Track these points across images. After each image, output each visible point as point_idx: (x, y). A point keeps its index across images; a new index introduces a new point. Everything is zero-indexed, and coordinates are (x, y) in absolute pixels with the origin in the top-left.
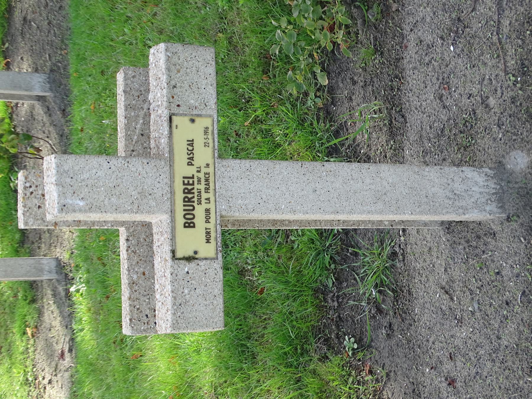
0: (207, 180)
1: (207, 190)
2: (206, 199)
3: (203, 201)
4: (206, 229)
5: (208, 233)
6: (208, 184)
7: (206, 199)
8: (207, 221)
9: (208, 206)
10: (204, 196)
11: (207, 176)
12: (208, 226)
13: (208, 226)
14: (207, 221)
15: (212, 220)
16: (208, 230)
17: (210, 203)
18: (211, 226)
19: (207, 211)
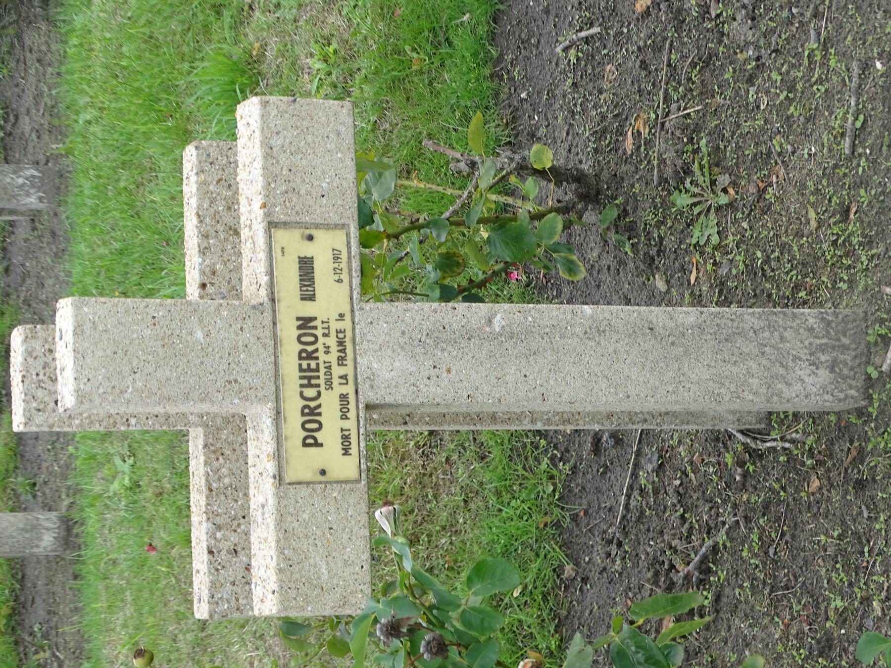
0: (341, 343)
1: (341, 361)
2: (341, 377)
3: (336, 381)
4: (342, 430)
5: (346, 438)
6: (343, 351)
7: (341, 377)
8: (344, 417)
9: (344, 390)
10: (337, 371)
11: (341, 335)
12: (346, 424)
13: (346, 424)
14: (344, 417)
15: (352, 414)
16: (346, 433)
17: (347, 383)
18: (351, 424)
19: (344, 397)
